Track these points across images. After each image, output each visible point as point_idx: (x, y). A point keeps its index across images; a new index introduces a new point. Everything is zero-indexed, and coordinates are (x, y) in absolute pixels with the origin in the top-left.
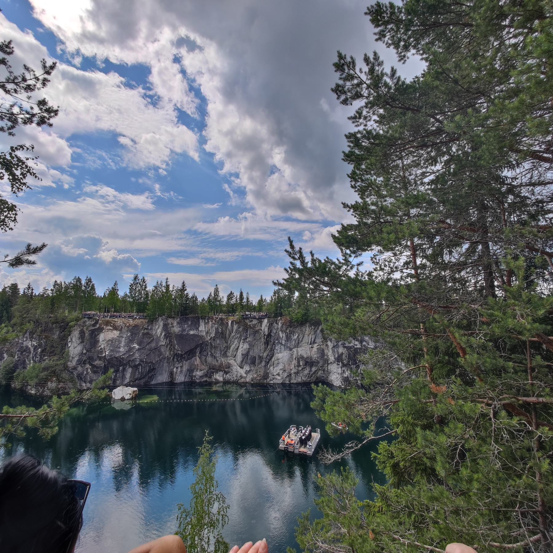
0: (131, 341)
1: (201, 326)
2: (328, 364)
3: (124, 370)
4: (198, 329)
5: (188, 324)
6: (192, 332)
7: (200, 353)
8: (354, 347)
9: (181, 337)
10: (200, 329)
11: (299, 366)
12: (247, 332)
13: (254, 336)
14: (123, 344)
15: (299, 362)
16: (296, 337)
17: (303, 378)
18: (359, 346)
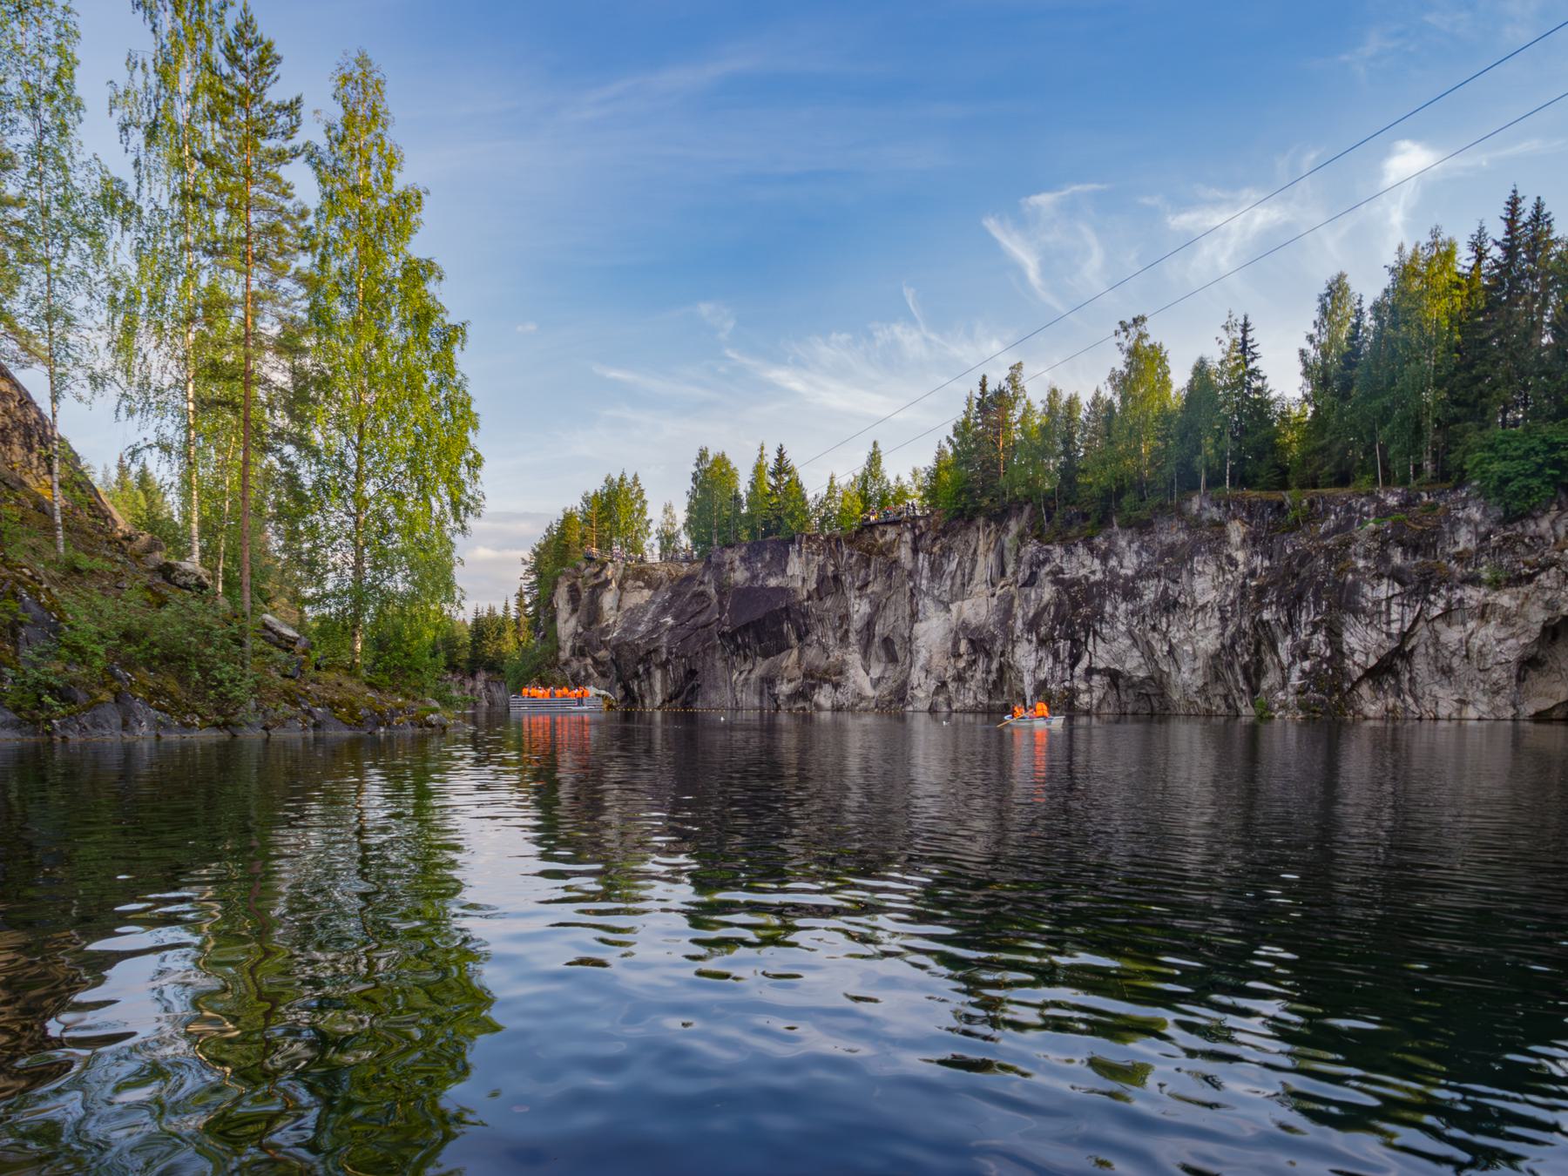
0: (664, 610)
1: (791, 564)
2: (1014, 643)
3: (648, 672)
4: (784, 571)
5: (763, 560)
6: (772, 582)
7: (800, 638)
8: (1087, 578)
9: (746, 595)
10: (789, 572)
11: (957, 656)
12: (868, 566)
13: (889, 576)
14: (649, 615)
15: (956, 644)
16: (953, 565)
17: (980, 697)
18: (1099, 576)
